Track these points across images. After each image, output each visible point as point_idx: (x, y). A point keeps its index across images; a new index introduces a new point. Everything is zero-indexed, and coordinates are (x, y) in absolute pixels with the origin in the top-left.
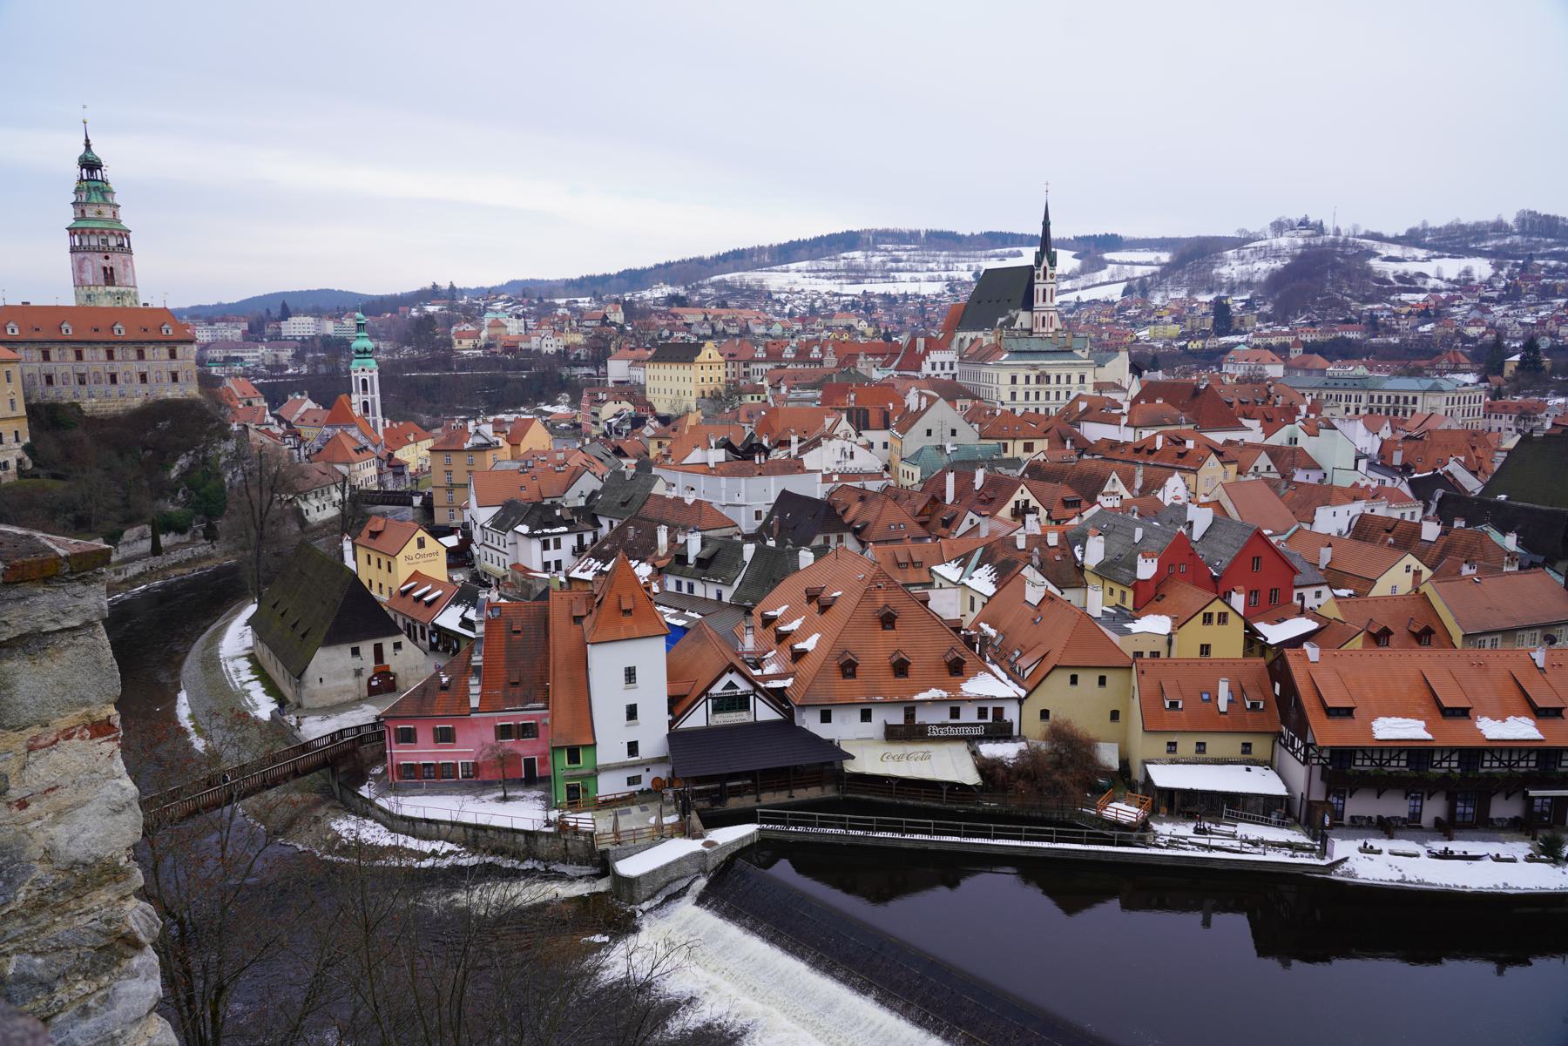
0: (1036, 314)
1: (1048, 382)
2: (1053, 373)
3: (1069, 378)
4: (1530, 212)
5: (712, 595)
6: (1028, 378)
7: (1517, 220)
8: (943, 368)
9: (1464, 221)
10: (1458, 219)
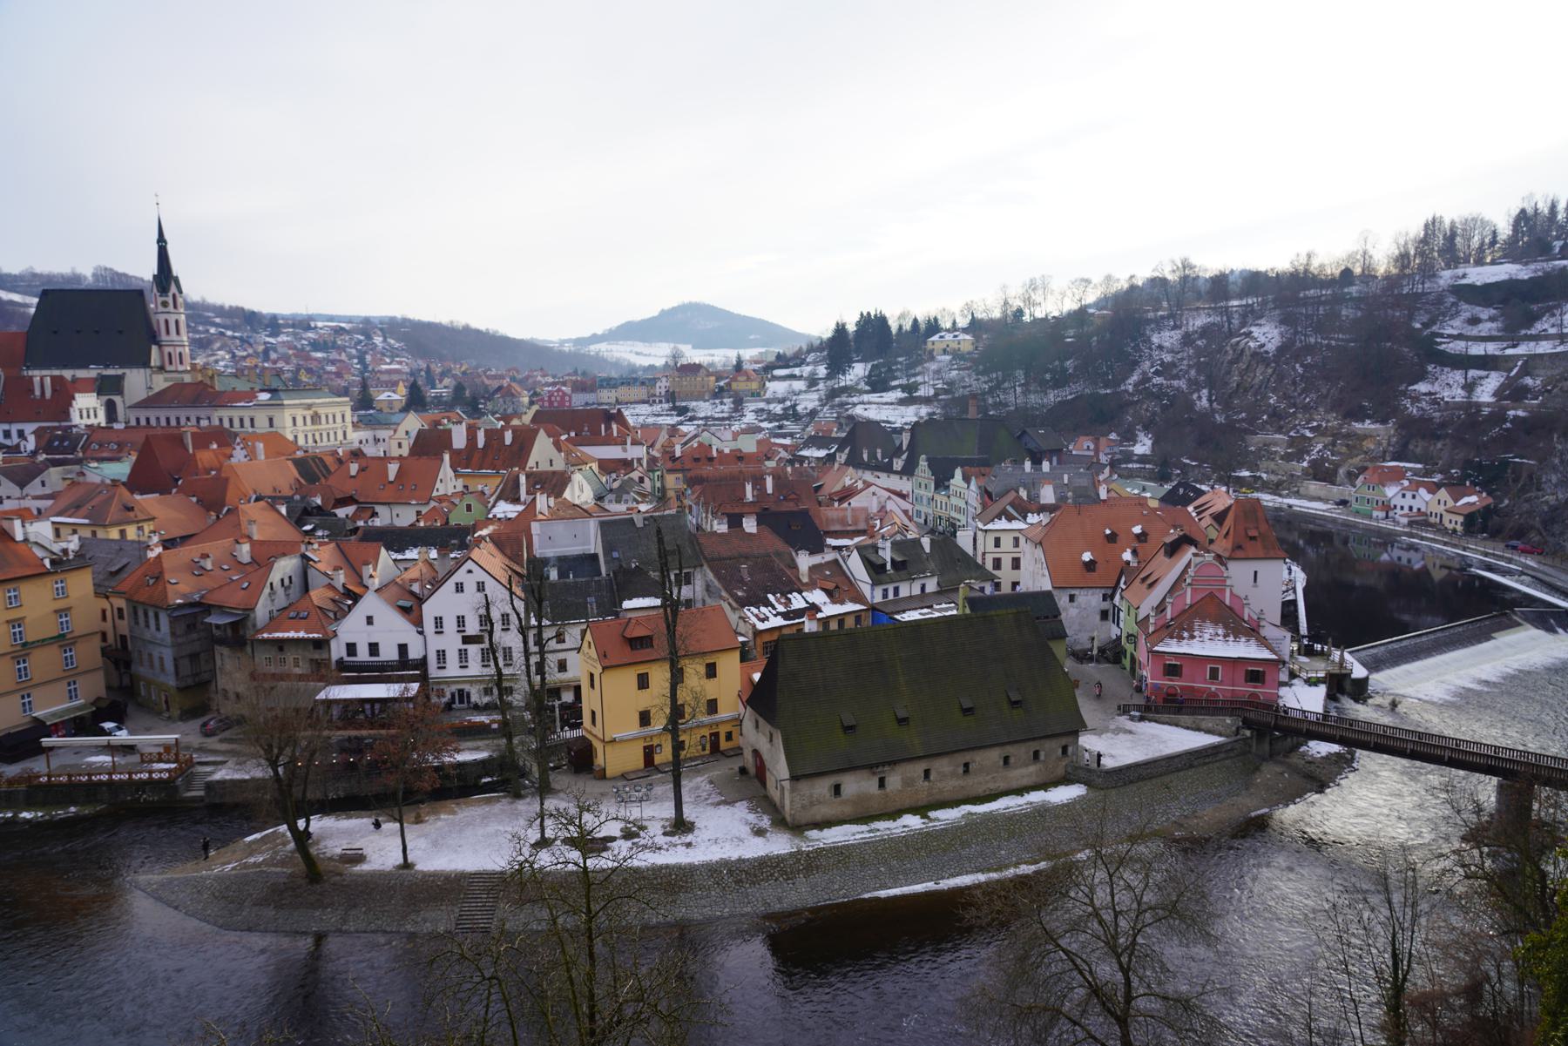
0: (167, 350)
1: (320, 424)
2: (322, 411)
3: (334, 416)
4: (106, 269)
5: (916, 591)
6: (304, 418)
7: (94, 275)
8: (88, 417)
9: (38, 270)
10: (32, 268)
